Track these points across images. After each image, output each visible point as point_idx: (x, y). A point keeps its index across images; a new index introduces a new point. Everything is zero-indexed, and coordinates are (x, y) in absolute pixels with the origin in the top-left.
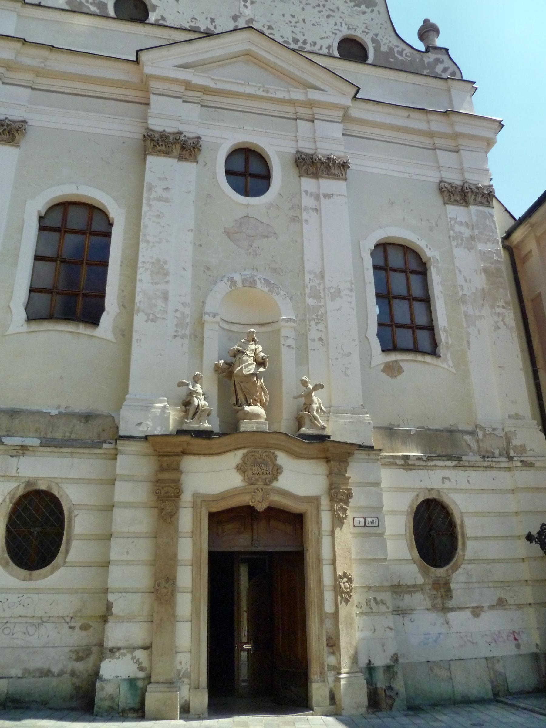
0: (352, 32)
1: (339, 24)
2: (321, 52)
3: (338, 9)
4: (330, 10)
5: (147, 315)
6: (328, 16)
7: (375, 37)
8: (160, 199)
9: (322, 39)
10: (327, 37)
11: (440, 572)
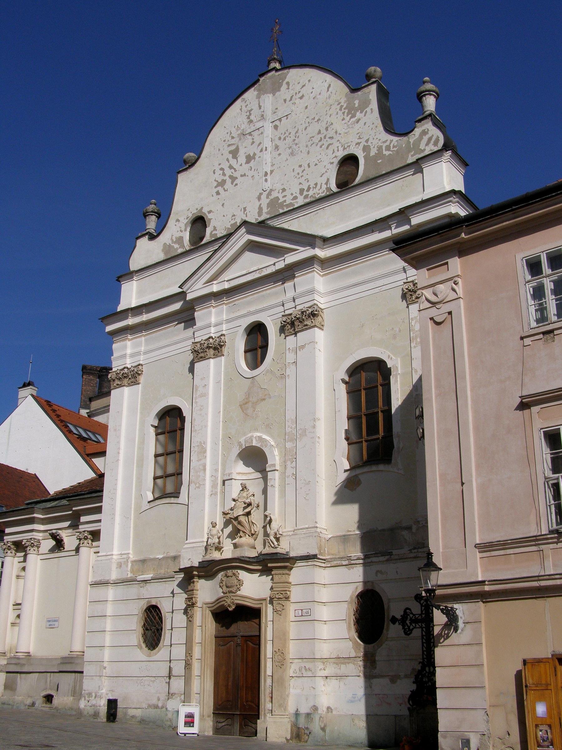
1: (336, 150)
6: (327, 148)
7: (366, 144)
10: (326, 172)
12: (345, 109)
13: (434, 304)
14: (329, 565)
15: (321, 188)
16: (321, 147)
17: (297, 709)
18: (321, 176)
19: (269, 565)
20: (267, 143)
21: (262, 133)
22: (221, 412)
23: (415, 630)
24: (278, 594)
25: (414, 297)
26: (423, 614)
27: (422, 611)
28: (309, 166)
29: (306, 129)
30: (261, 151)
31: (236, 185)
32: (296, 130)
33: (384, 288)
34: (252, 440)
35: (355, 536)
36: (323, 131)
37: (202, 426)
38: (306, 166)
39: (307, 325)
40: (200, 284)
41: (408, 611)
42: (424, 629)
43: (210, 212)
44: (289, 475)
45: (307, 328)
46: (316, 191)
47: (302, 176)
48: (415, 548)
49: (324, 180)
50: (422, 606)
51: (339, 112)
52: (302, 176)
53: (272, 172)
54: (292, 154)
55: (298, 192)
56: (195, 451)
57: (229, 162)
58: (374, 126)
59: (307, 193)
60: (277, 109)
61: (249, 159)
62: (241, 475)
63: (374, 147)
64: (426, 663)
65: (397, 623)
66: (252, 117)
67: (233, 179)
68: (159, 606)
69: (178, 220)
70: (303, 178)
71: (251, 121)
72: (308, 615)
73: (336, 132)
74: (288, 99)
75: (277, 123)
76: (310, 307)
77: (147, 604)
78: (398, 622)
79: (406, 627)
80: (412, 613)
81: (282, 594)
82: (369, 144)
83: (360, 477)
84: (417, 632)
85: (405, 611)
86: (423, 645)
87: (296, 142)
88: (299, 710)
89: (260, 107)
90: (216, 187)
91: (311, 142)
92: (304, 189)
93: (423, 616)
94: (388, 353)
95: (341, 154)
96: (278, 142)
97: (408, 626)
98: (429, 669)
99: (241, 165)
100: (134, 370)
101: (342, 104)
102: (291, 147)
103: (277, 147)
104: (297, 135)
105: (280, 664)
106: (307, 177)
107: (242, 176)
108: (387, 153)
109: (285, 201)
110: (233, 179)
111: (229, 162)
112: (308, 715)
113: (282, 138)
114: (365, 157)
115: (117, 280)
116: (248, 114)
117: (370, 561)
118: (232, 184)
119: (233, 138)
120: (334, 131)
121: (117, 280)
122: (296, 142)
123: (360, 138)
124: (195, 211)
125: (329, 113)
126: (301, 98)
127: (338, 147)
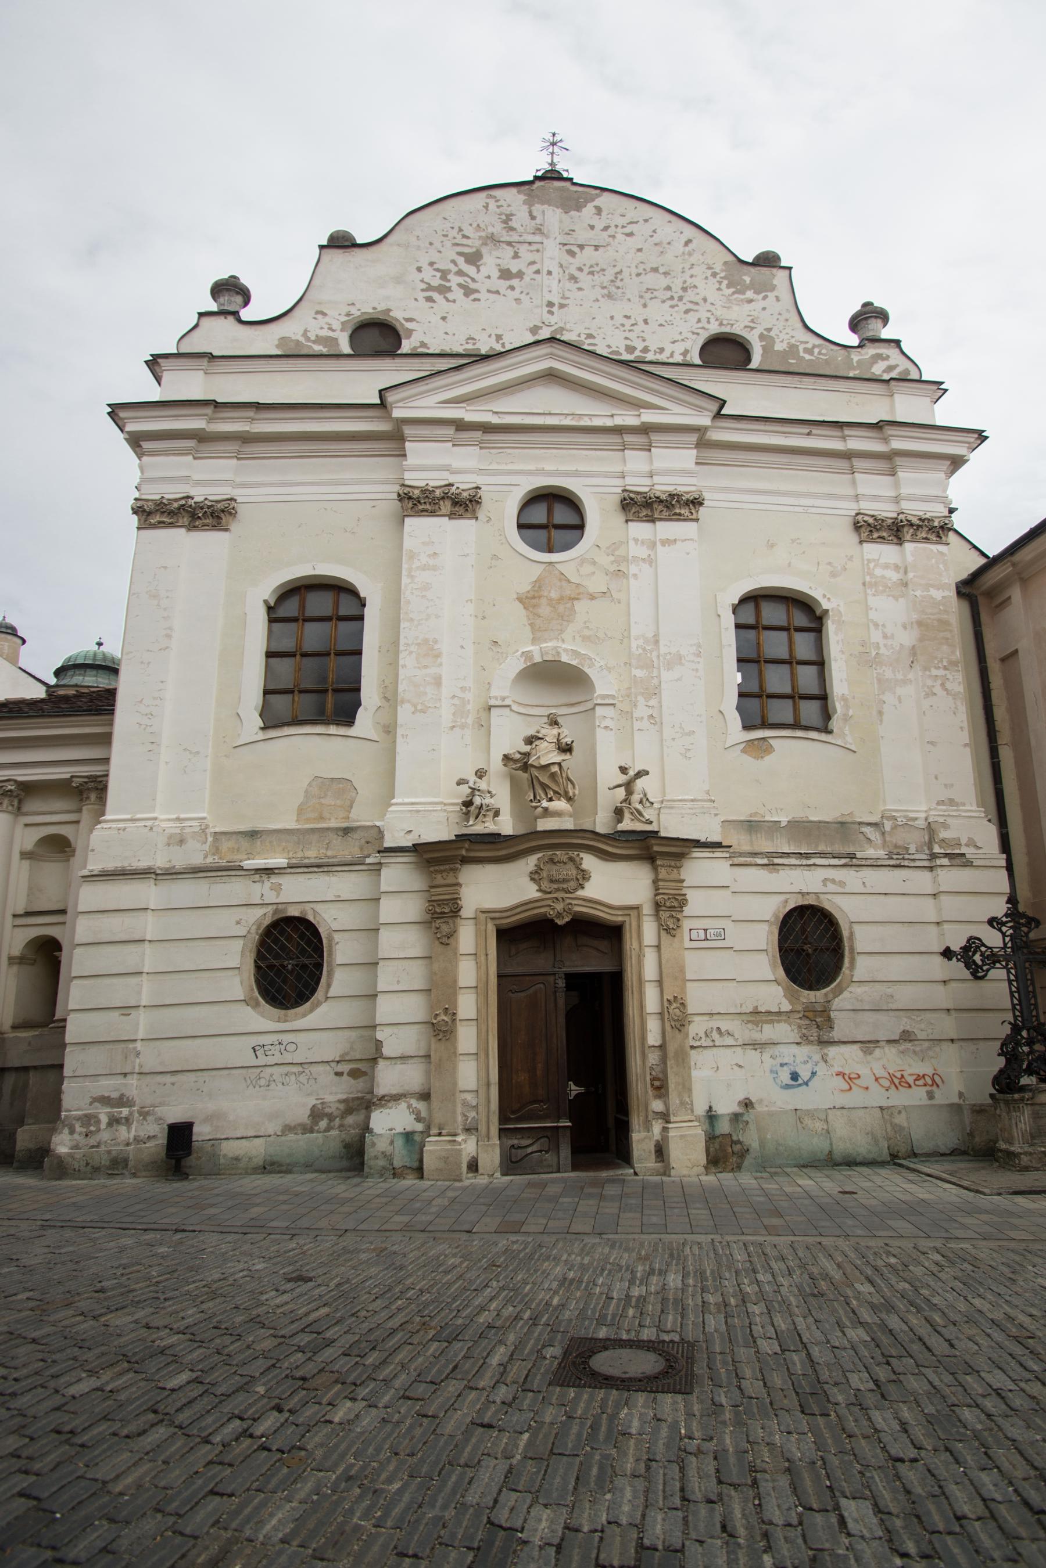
2: (671, 360)
3: (705, 300)
4: (691, 302)
5: (415, 706)
8: (425, 568)
9: (674, 342)
11: (815, 996)
17: (710, 1107)
19: (656, 848)
29: (638, 275)
32: (617, 269)
45: (679, 518)
56: (411, 653)
104: (620, 277)
105: (678, 1024)
112: (736, 1117)
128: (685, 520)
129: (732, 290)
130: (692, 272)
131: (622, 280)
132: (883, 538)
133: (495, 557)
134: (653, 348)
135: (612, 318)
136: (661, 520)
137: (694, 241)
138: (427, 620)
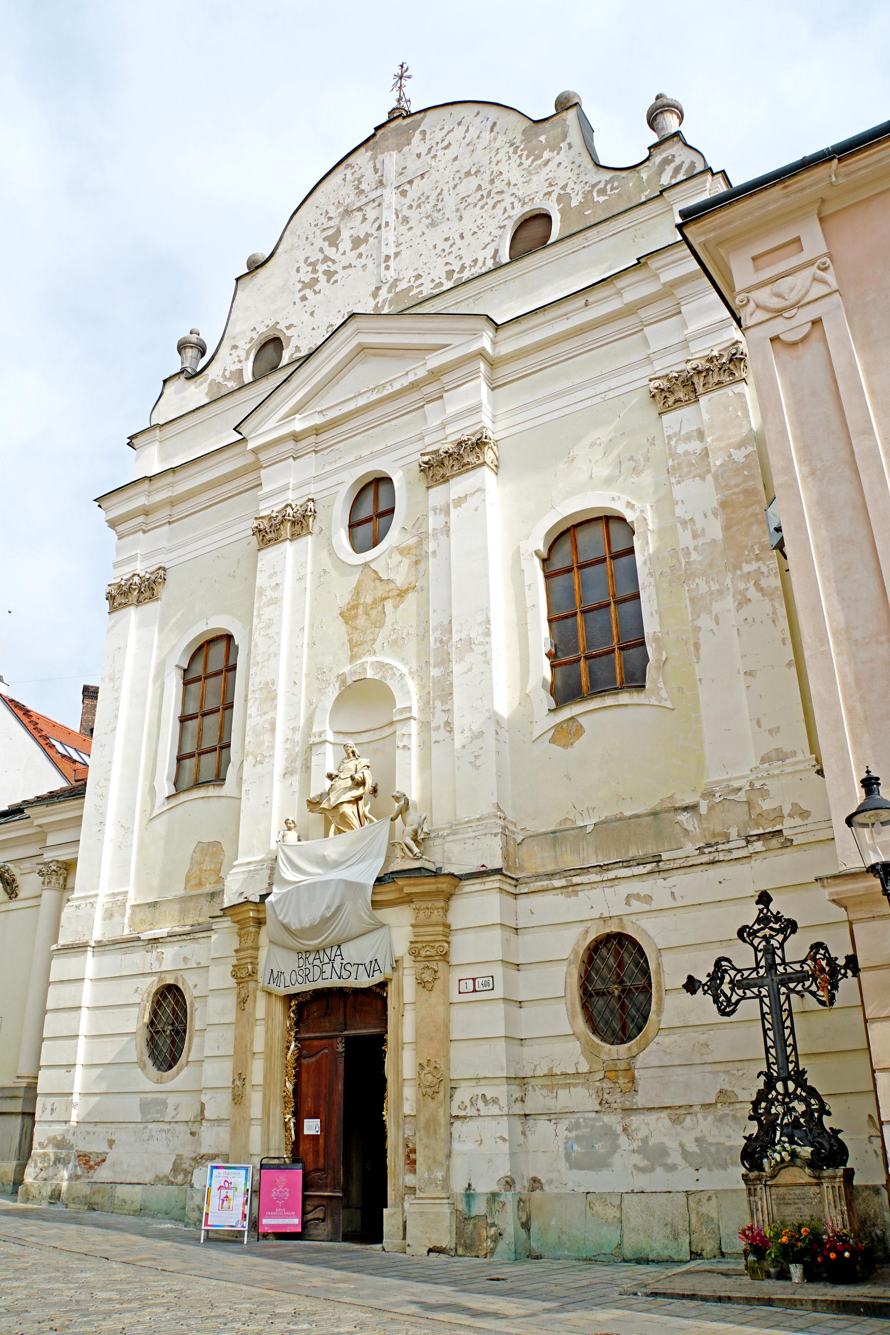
0: (527, 208)
1: (509, 207)
6: (494, 207)
7: (562, 192)
10: (493, 241)
12: (522, 150)
13: (779, 312)
14: (526, 890)
15: (484, 264)
16: (482, 207)
17: (470, 1185)
18: (484, 248)
19: (407, 890)
20: (389, 216)
21: (380, 205)
22: (306, 629)
23: (742, 1002)
24: (423, 947)
25: (671, 401)
26: (762, 967)
27: (758, 963)
28: (462, 237)
29: (455, 186)
30: (379, 228)
31: (336, 281)
32: (439, 190)
33: (612, 394)
34: (365, 669)
35: (576, 831)
36: (486, 185)
37: (269, 655)
38: (457, 237)
39: (468, 463)
40: (272, 423)
41: (724, 963)
42: (766, 1000)
43: (288, 328)
44: (439, 726)
45: (467, 468)
46: (473, 270)
47: (449, 254)
48: (709, 845)
49: (490, 251)
50: (756, 949)
51: (512, 156)
52: (449, 254)
53: (397, 254)
54: (433, 224)
55: (444, 276)
56: (256, 699)
57: (323, 252)
58: (575, 166)
59: (460, 276)
60: (405, 168)
61: (357, 242)
62: (341, 736)
63: (577, 194)
64: (775, 1074)
65: (700, 990)
66: (363, 186)
67: (329, 274)
68: (181, 987)
69: (235, 347)
70: (452, 256)
71: (362, 191)
72: (487, 988)
73: (509, 184)
74: (424, 152)
75: (407, 187)
76: (473, 435)
77: (159, 982)
78: (701, 989)
79: (722, 998)
80: (734, 968)
81: (433, 947)
82: (568, 190)
83: (581, 720)
84: (749, 1009)
85: (718, 963)
86: (765, 1034)
87: (438, 207)
88: (473, 1187)
89: (376, 171)
90: (300, 291)
91: (465, 204)
92: (454, 271)
93: (762, 972)
94: (625, 498)
95: (519, 212)
96: (406, 212)
97: (725, 995)
98: (786, 1087)
99: (344, 253)
100: (149, 578)
101: (517, 145)
102: (430, 216)
103: (406, 220)
104: (440, 197)
106: (460, 252)
107: (344, 268)
108: (601, 199)
109: (421, 292)
110: (329, 274)
111: (323, 252)
113: (415, 205)
114: (561, 211)
115: (128, 444)
116: (356, 183)
117: (613, 877)
118: (328, 281)
119: (330, 218)
120: (506, 182)
121: (128, 444)
122: (438, 207)
123: (551, 185)
124: (265, 330)
125: (495, 160)
126: (446, 148)
127: (512, 203)
128: (473, 468)
129: (532, 158)
130: (498, 157)
131: (442, 200)
132: (679, 400)
133: (325, 571)
134: (468, 262)
135: (435, 247)
136: (453, 476)
137: (498, 123)
138: (268, 660)
